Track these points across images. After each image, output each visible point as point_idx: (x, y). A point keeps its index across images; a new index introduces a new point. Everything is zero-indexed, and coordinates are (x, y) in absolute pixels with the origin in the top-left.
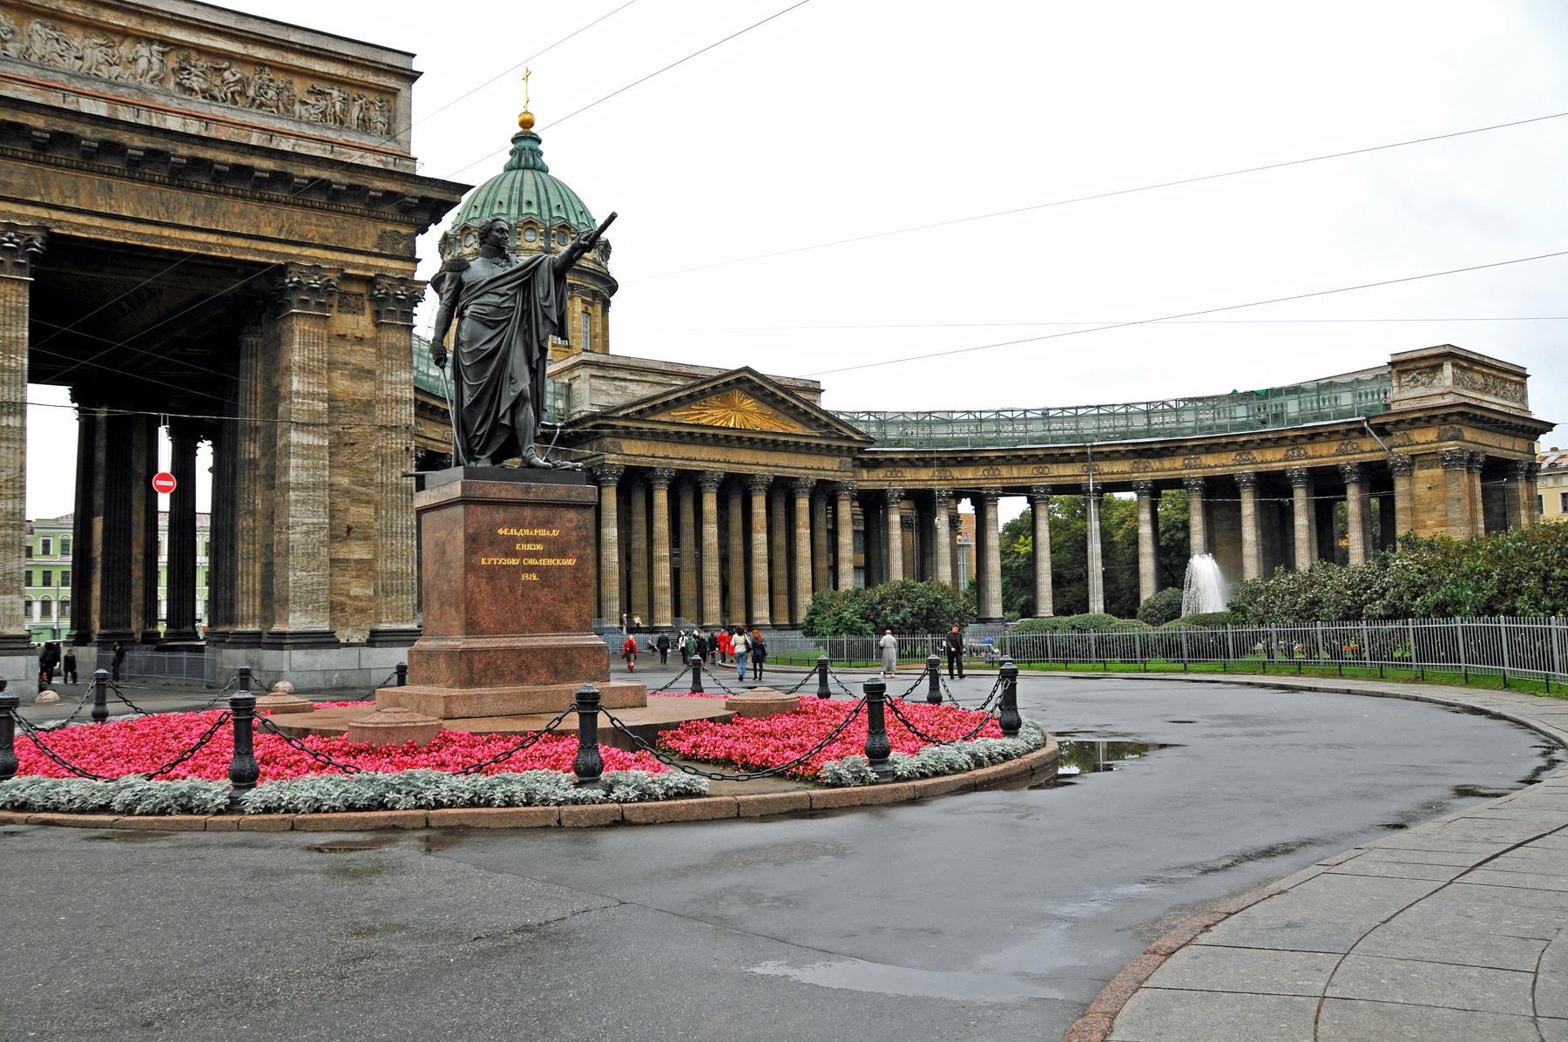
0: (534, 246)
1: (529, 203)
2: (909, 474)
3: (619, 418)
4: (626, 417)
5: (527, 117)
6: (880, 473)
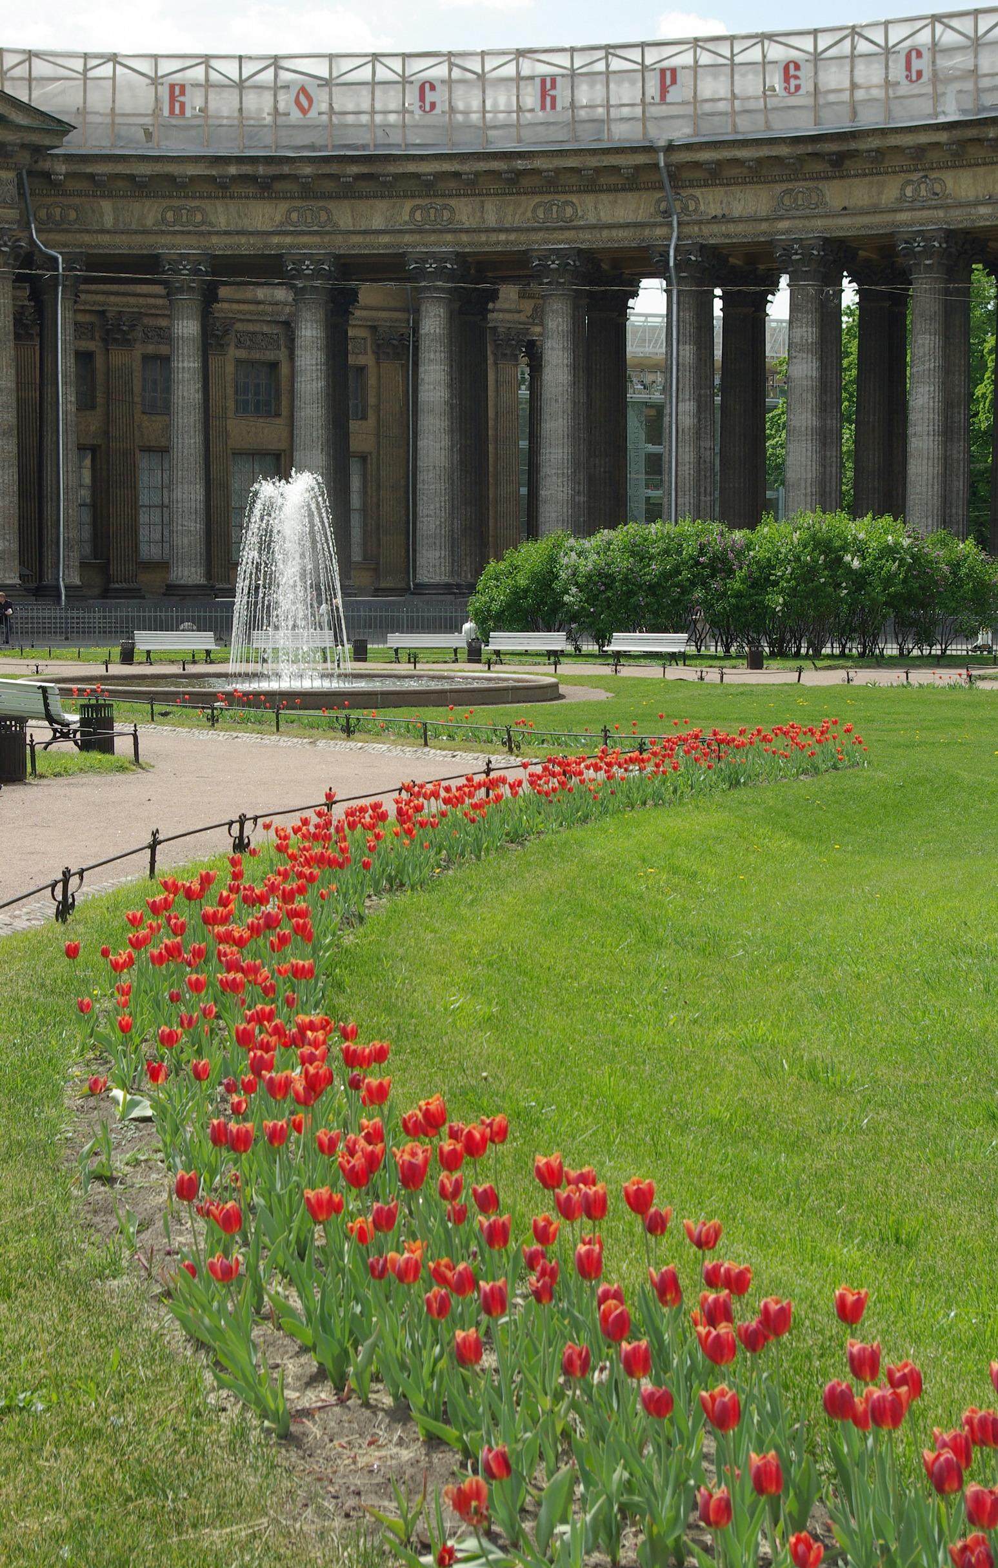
2: (222, 215)
6: (149, 212)
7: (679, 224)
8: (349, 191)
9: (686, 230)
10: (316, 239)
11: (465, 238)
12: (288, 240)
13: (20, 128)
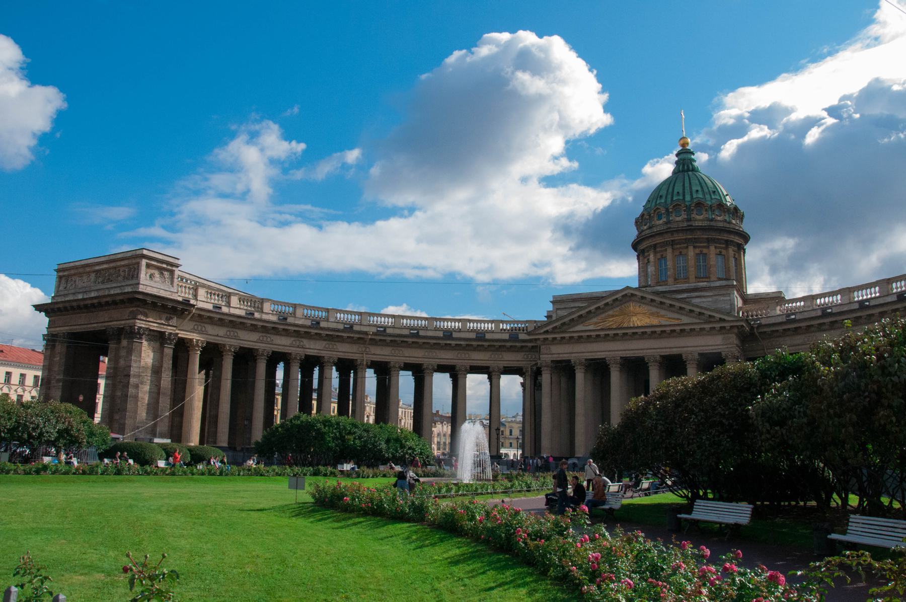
0: (661, 222)
1: (661, 197)
3: (540, 334)
4: (547, 332)
5: (682, 142)
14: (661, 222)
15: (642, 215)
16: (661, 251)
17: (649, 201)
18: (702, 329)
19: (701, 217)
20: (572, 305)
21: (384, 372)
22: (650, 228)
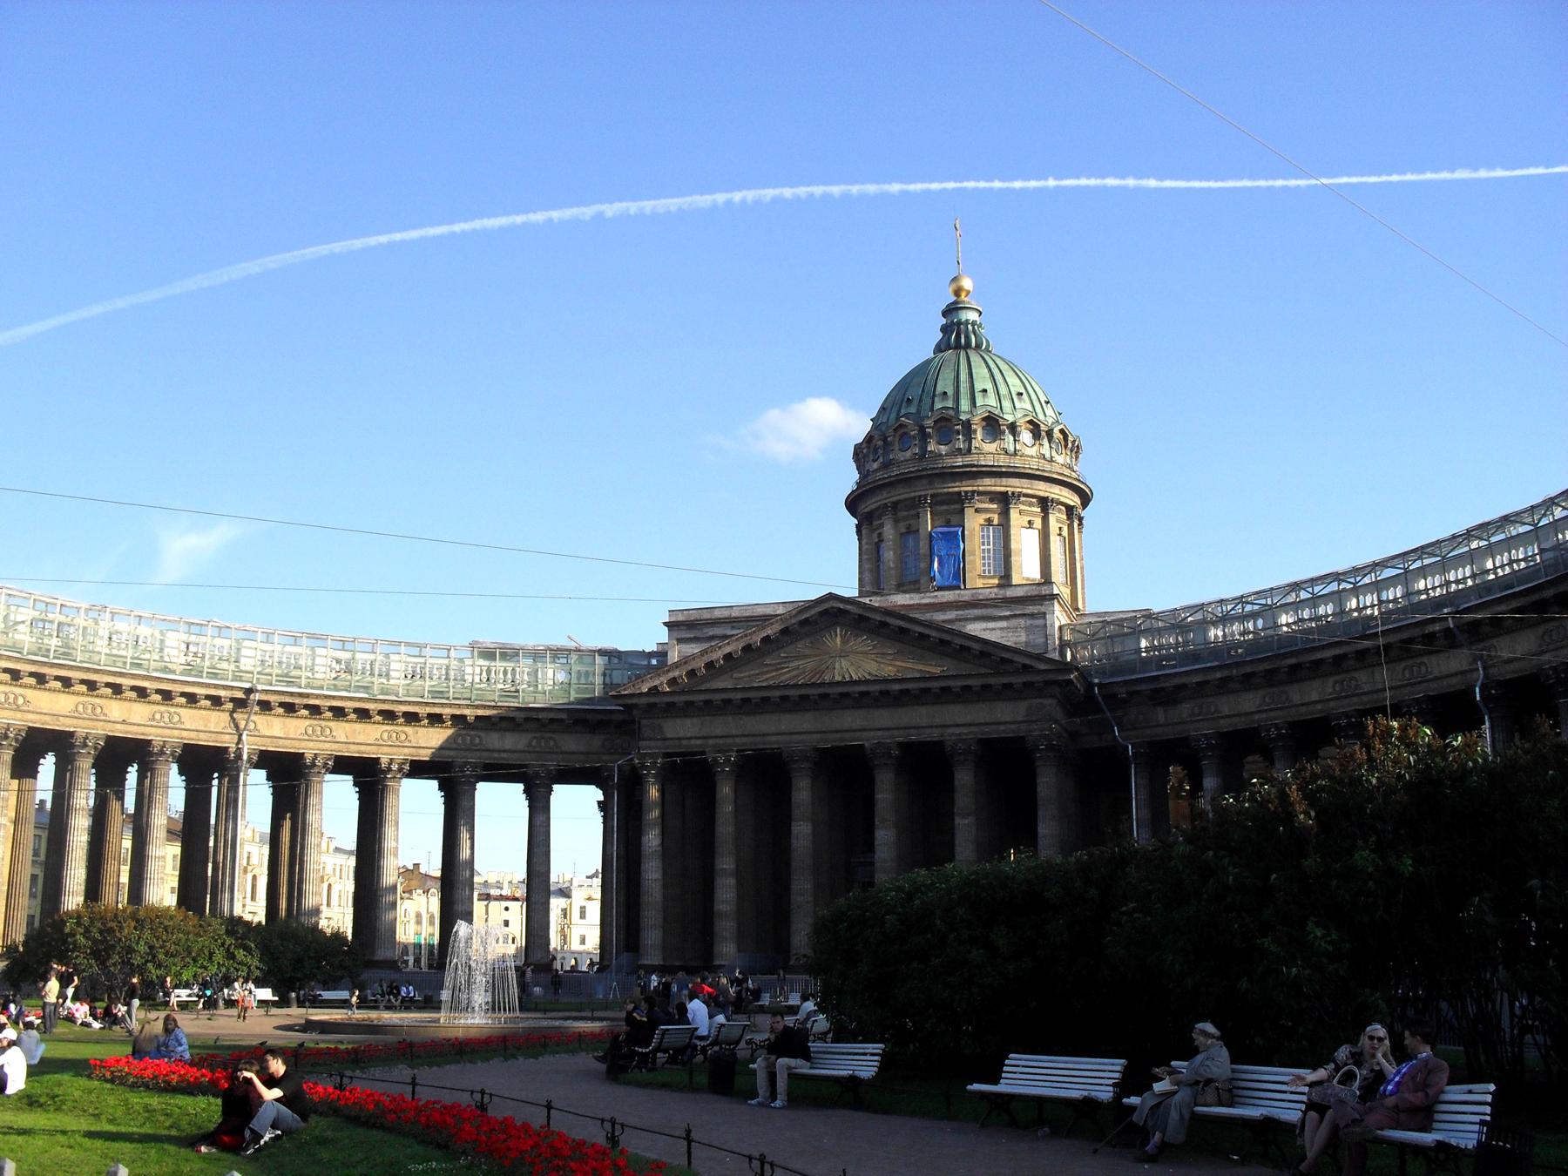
0: (908, 454)
5: (954, 286)
6: (1185, 709)
7: (1484, 668)
8: (1297, 673)
9: (1491, 671)
10: (1280, 713)
11: (1365, 698)
12: (1264, 716)
13: (1040, 671)
14: (908, 454)
15: (869, 439)
16: (905, 519)
17: (883, 409)
18: (986, 687)
19: (990, 447)
20: (712, 632)
21: (291, 778)
22: (886, 466)
